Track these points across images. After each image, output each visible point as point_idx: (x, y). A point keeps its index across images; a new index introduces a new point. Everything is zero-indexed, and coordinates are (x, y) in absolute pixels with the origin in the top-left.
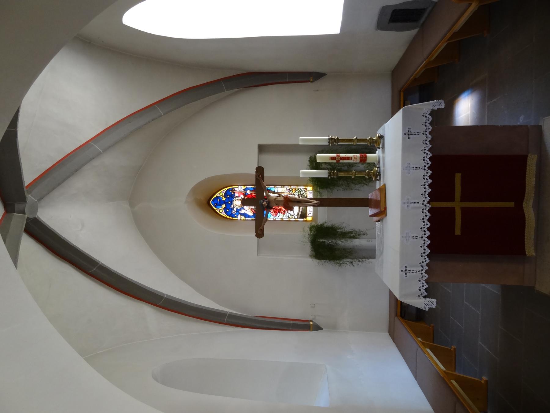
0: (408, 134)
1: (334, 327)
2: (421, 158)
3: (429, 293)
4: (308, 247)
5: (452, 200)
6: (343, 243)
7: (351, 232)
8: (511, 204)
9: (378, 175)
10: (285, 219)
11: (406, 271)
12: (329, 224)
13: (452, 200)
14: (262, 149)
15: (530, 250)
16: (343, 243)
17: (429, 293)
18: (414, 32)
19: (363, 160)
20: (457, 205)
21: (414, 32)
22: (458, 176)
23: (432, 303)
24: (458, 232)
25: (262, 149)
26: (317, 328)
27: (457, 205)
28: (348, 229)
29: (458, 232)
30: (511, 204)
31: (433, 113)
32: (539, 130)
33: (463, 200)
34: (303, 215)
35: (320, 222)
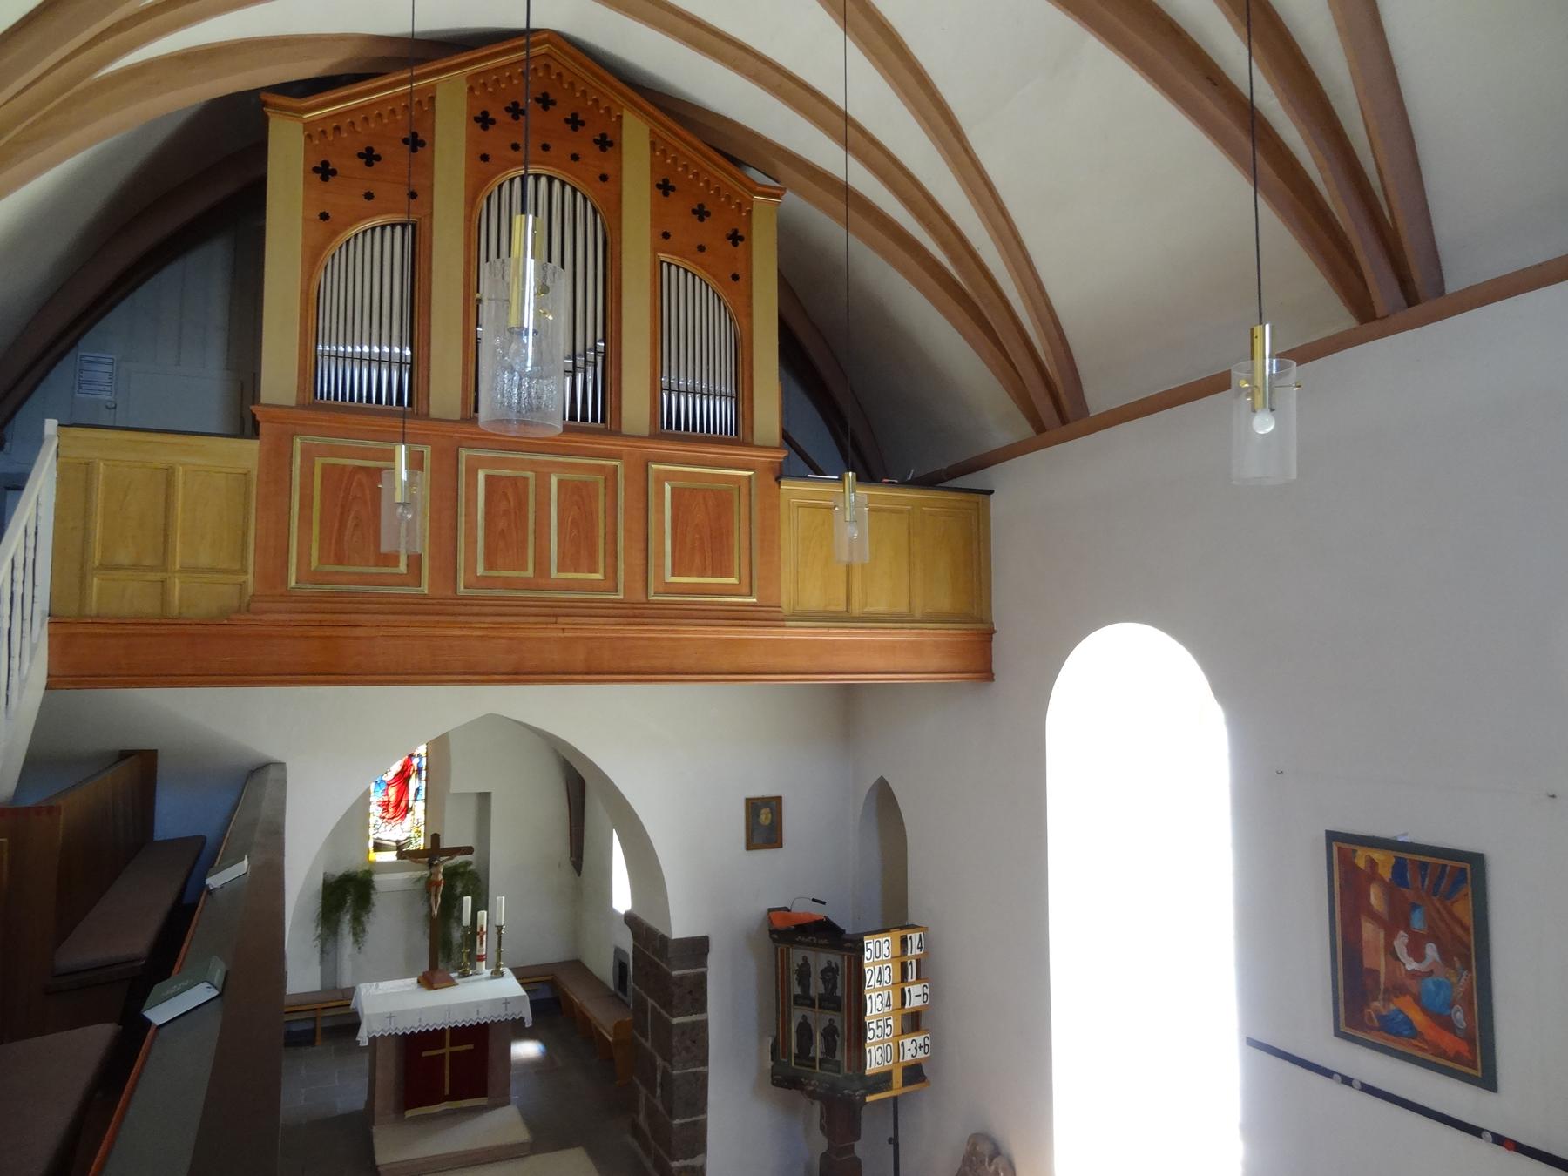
0: (506, 1002)
2: (485, 1016)
4: (339, 871)
5: (452, 1045)
6: (347, 918)
7: (363, 931)
8: (447, 1092)
9: (464, 975)
10: (372, 820)
11: (391, 1017)
12: (374, 898)
13: (452, 1045)
14: (484, 798)
15: (409, 1114)
16: (347, 918)
17: (373, 1040)
18: (612, 986)
19: (481, 958)
20: (447, 1050)
21: (612, 986)
24: (425, 1054)
25: (484, 798)
28: (368, 927)
29: (425, 1054)
31: (522, 1019)
32: (507, 1103)
34: (378, 847)
35: (377, 878)
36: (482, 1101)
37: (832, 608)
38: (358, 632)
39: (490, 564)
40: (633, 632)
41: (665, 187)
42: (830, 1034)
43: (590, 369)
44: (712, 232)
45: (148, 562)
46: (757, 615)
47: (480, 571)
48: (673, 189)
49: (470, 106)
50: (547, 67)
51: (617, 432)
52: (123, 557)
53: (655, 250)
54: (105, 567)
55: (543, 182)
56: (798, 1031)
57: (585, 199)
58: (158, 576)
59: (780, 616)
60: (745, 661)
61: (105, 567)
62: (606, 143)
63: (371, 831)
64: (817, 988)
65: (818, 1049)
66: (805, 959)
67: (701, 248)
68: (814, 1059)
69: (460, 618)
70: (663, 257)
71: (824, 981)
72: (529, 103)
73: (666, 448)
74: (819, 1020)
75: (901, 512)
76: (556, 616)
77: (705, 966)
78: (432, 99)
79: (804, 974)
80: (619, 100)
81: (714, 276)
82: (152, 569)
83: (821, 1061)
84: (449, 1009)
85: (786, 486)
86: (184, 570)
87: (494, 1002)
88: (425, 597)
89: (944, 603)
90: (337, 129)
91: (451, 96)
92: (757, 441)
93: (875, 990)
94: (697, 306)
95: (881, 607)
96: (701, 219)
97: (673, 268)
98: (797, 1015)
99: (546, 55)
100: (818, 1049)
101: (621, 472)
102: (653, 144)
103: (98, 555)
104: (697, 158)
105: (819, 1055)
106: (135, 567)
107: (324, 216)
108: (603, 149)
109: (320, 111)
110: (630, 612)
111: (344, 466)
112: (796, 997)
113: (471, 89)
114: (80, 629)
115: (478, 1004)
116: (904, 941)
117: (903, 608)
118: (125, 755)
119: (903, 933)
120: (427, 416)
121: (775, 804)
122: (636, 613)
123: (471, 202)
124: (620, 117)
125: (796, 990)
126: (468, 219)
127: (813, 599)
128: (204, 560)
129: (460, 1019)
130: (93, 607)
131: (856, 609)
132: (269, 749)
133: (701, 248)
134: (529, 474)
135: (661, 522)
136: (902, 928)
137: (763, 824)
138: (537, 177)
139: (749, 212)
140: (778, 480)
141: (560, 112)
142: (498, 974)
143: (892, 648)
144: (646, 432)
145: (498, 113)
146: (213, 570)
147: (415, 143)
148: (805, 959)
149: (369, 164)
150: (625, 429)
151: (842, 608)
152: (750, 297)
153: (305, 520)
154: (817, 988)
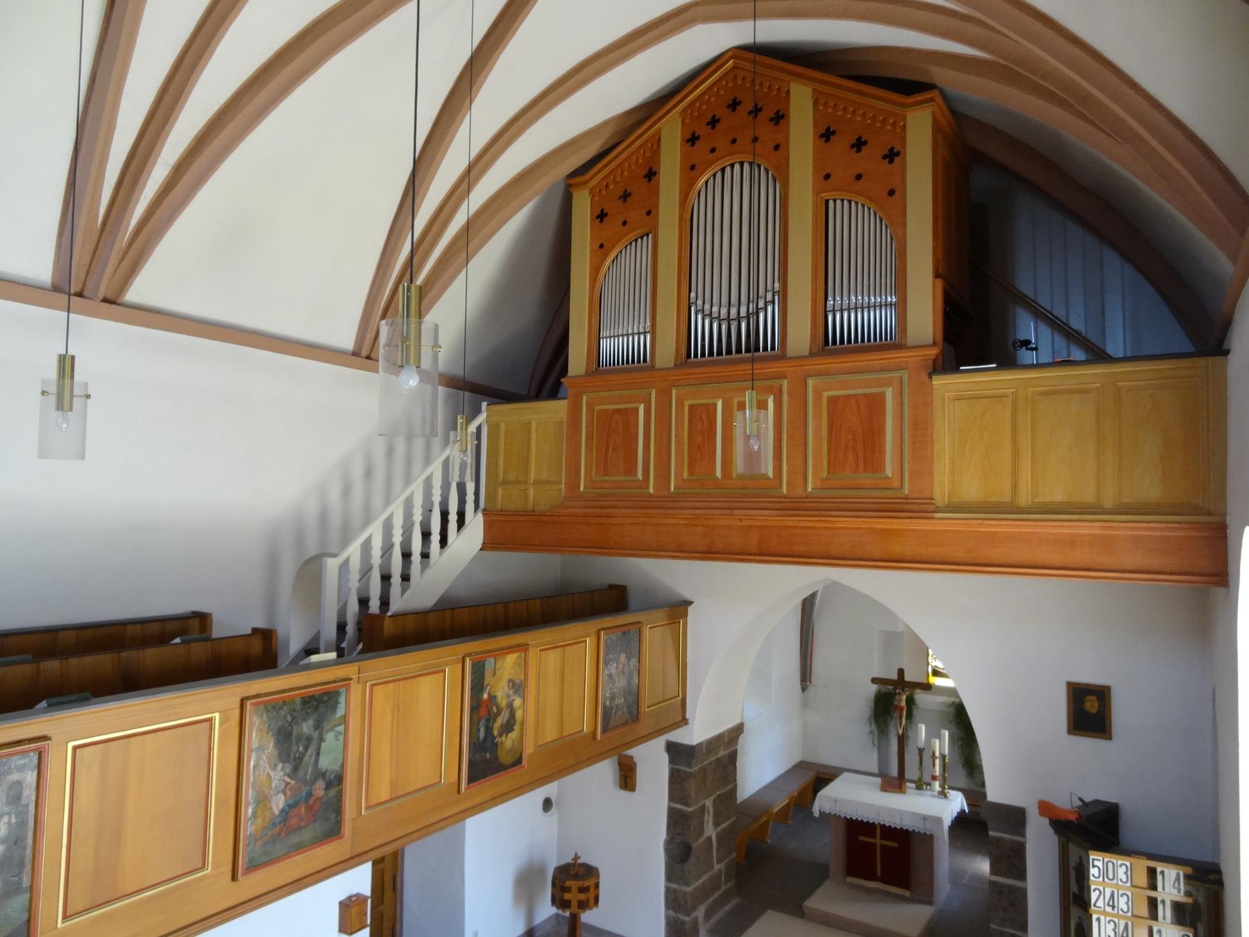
0: (925, 818)
1: (805, 705)
2: (908, 824)
3: (822, 813)
8: (879, 874)
11: (836, 801)
15: (851, 880)
19: (934, 778)
22: (896, 845)
23: (816, 814)
24: (861, 838)
26: (804, 689)
27: (878, 841)
30: (879, 874)
33: (882, 846)
34: (936, 673)
36: (907, 893)
37: (995, 499)
38: (615, 521)
39: (691, 473)
40: (791, 521)
41: (827, 135)
43: (769, 309)
44: (869, 159)
45: (521, 479)
46: (906, 507)
47: (686, 475)
48: (834, 133)
49: (683, 133)
50: (735, 76)
51: (783, 356)
52: (511, 477)
53: (817, 192)
54: (504, 482)
55: (737, 167)
57: (767, 171)
58: (522, 487)
59: (932, 508)
60: (897, 548)
61: (504, 482)
62: (780, 118)
63: (930, 660)
67: (859, 177)
69: (669, 511)
70: (825, 195)
72: (722, 112)
73: (822, 364)
75: (1086, 391)
76: (732, 509)
77: (1023, 835)
78: (659, 139)
80: (782, 76)
81: (869, 198)
82: (517, 482)
84: (892, 811)
85: (938, 381)
86: (536, 482)
87: (914, 814)
88: (651, 496)
89: (1149, 488)
90: (607, 185)
91: (671, 130)
92: (910, 342)
93: (1105, 914)
94: (857, 224)
95: (1057, 495)
96: (859, 151)
97: (838, 202)
99: (735, 67)
101: (785, 389)
102: (816, 103)
103: (501, 476)
104: (854, 97)
106: (517, 482)
107: (601, 246)
108: (777, 123)
109: (596, 177)
110: (791, 505)
111: (607, 411)
112: (1074, 894)
113: (683, 122)
114: (494, 518)
115: (901, 813)
116: (1152, 873)
117: (1087, 495)
118: (611, 587)
119: (1152, 864)
120: (652, 367)
121: (1102, 694)
122: (795, 506)
123: (683, 203)
124: (788, 92)
126: (681, 218)
127: (972, 490)
128: (544, 476)
129: (895, 822)
130: (499, 506)
131: (1024, 499)
132: (686, 593)
133: (859, 177)
134: (687, 404)
135: (818, 428)
136: (1151, 857)
137: (1089, 711)
138: (732, 166)
139: (904, 125)
140: (930, 376)
141: (742, 110)
142: (943, 794)
143: (1072, 542)
144: (806, 352)
145: (702, 130)
146: (548, 482)
147: (651, 174)
149: (625, 201)
150: (790, 352)
151: (1007, 498)
152: (905, 208)
153: (589, 449)
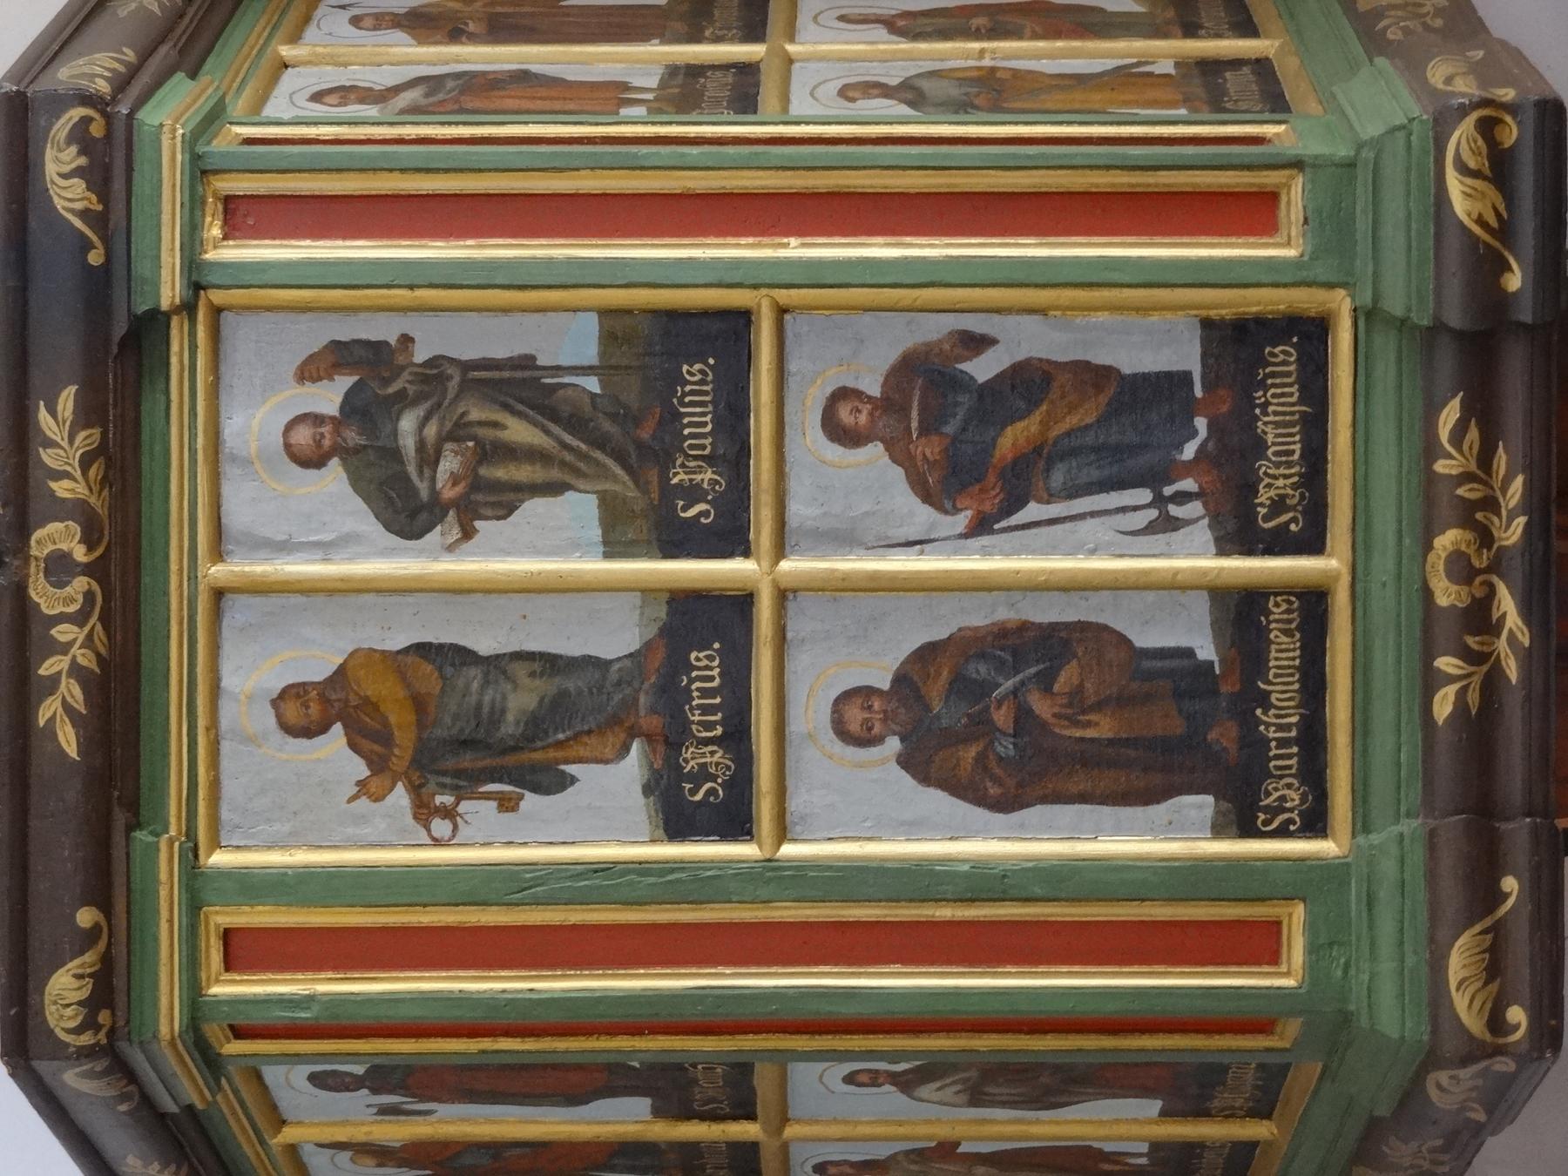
42: (974, 432)
56: (1005, 789)
64: (552, 571)
65: (1127, 563)
66: (307, 710)
68: (1241, 610)
71: (483, 501)
74: (864, 557)
79: (447, 725)
83: (1240, 535)
98: (861, 819)
100: (1127, 563)
105: (1196, 558)
125: (598, 822)
148: (307, 710)
154: (552, 571)
